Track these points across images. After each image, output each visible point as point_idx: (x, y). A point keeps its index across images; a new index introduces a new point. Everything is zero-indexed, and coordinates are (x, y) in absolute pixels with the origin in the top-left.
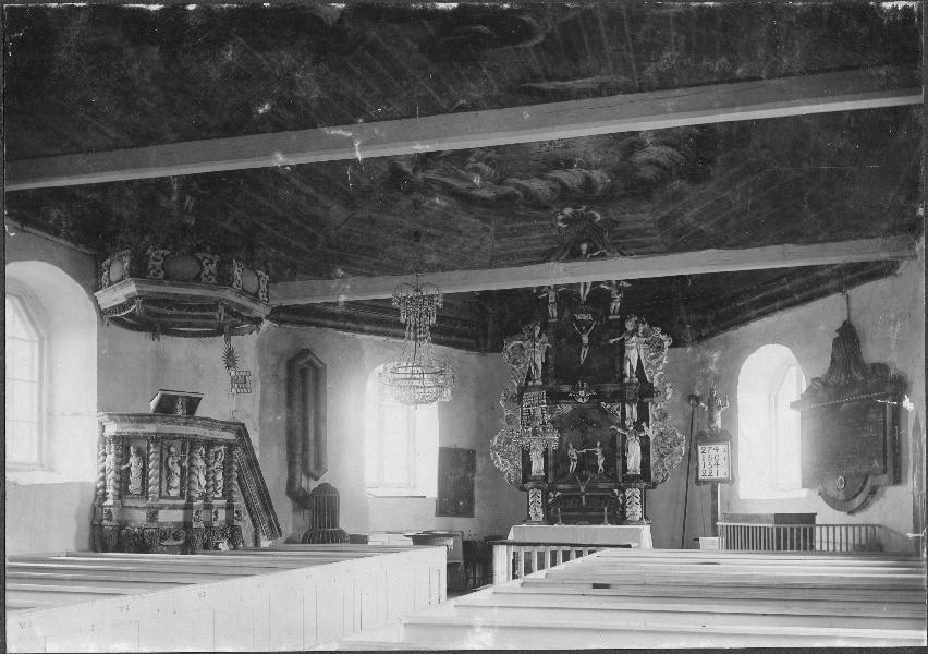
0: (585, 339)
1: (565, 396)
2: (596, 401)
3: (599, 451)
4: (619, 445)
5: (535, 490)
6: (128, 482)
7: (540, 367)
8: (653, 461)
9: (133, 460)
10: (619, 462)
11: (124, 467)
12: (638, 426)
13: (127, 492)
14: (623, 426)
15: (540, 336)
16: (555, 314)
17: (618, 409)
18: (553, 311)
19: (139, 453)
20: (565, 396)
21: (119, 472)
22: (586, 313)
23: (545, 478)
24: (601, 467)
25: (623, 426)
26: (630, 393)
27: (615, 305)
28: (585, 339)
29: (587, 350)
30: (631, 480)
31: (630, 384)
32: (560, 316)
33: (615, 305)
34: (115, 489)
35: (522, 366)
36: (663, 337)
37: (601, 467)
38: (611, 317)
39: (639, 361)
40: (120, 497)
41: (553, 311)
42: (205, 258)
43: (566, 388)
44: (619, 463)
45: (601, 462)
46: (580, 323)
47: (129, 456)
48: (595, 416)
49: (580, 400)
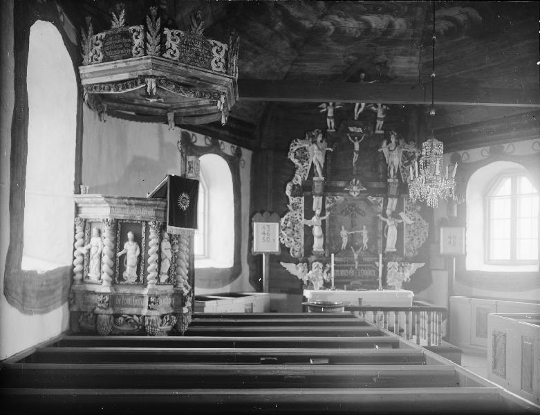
1: (341, 190)
3: (365, 233)
4: (380, 228)
5: (318, 263)
6: (122, 269)
7: (322, 165)
8: (406, 240)
9: (130, 249)
10: (380, 242)
11: (119, 254)
13: (121, 278)
14: (385, 215)
15: (321, 142)
16: (333, 125)
18: (330, 123)
19: (137, 239)
21: (114, 258)
22: (358, 127)
24: (365, 245)
25: (385, 215)
27: (380, 123)
30: (388, 257)
31: (394, 183)
33: (380, 123)
34: (108, 273)
35: (305, 164)
37: (365, 245)
38: (377, 132)
40: (113, 284)
41: (330, 123)
42: (215, 45)
44: (380, 242)
45: (365, 241)
46: (353, 135)
47: (124, 239)
49: (352, 194)
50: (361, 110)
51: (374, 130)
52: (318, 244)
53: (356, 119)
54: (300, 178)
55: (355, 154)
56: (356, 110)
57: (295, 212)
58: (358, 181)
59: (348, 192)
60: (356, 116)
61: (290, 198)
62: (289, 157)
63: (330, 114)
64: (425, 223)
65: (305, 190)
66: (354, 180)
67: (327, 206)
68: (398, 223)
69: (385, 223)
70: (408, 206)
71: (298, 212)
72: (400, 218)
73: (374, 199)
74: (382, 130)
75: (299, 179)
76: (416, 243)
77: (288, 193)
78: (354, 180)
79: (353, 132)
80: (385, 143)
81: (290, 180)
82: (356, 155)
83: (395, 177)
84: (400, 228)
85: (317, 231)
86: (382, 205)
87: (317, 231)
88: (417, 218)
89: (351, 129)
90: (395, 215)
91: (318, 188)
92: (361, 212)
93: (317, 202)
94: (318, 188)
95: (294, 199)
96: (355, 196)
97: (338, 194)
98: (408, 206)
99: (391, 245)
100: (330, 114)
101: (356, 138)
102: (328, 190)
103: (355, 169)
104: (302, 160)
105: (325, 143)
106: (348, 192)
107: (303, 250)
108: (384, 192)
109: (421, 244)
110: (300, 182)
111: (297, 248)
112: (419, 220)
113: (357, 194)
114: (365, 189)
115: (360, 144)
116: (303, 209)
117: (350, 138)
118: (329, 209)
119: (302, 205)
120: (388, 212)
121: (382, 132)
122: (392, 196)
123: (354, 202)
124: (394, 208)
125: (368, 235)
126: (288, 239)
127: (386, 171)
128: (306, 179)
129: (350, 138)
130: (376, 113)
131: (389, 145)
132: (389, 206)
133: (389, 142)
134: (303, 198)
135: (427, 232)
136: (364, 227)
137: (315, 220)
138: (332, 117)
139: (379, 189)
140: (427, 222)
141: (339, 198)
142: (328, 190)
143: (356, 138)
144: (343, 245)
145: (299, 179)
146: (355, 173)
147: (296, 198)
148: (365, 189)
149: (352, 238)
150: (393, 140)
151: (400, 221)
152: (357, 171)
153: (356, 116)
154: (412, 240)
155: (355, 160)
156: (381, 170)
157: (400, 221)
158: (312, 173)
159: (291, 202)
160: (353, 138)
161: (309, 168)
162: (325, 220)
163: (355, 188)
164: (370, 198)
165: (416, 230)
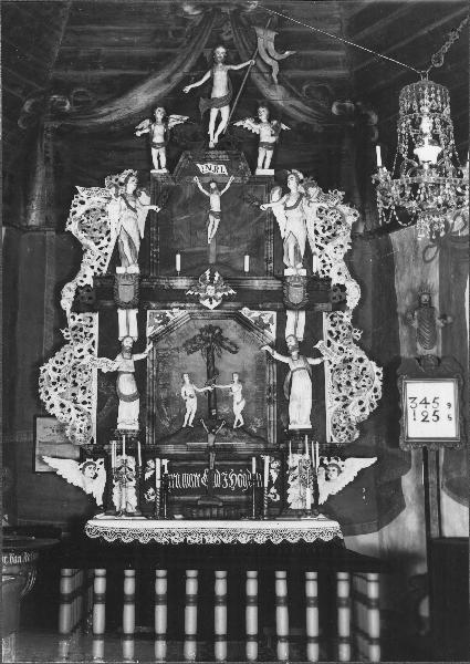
0: (215, 203)
1: (180, 296)
2: (233, 305)
8: (331, 406)
12: (307, 348)
14: (285, 352)
17: (271, 320)
18: (159, 156)
20: (180, 296)
23: (141, 435)
24: (239, 417)
26: (296, 295)
27: (265, 156)
28: (215, 203)
29: (217, 221)
32: (171, 164)
33: (265, 156)
35: (104, 243)
36: (345, 209)
37: (239, 417)
38: (259, 172)
39: (307, 243)
41: (159, 156)
43: (181, 283)
48: (232, 331)
49: (206, 303)
50: (223, 126)
51: (253, 166)
52: (128, 416)
53: (211, 145)
54: (90, 273)
55: (211, 218)
56: (211, 132)
57: (80, 346)
58: (217, 275)
59: (196, 299)
60: (214, 140)
61: (69, 314)
62: (69, 228)
63: (158, 139)
64: (373, 368)
65: (101, 298)
66: (208, 272)
67: (150, 331)
68: (312, 366)
69: (284, 369)
70: (333, 329)
71: (86, 345)
72: (318, 354)
73: (256, 314)
74: (270, 168)
75: (86, 276)
76: (355, 413)
77: (66, 304)
78: (208, 272)
79: (208, 175)
80: (276, 194)
81: (71, 277)
82: (213, 224)
83: (300, 265)
84: (317, 375)
85: (127, 386)
86: (273, 328)
87: (127, 386)
88: (357, 356)
89: (203, 168)
90: (307, 348)
91: (126, 293)
92: (227, 345)
93: (127, 322)
94: (126, 293)
95: (77, 317)
96: (211, 307)
97: (174, 304)
98: (333, 329)
99: (300, 417)
100: (158, 139)
101: (213, 185)
102: (148, 296)
103: (213, 249)
104: (97, 234)
105: (145, 198)
106: (196, 299)
107: (94, 433)
108: (278, 301)
109: (367, 412)
110: (89, 281)
111: (79, 424)
112: (361, 360)
113: (215, 304)
114: (232, 292)
115: (222, 198)
116: (96, 338)
117: (200, 187)
118: (156, 339)
119: (95, 330)
120: (291, 343)
121: (272, 172)
122: (296, 308)
123: (213, 323)
124: (300, 334)
125: (245, 394)
126: (62, 406)
127: (280, 252)
128: (105, 270)
129: (200, 187)
130: (257, 137)
131: (285, 197)
132: (289, 331)
133: (286, 191)
134: (96, 316)
135: (380, 389)
136: (236, 378)
137: (124, 363)
138: (162, 145)
139: (265, 292)
140: (378, 366)
141: (177, 314)
142: (148, 296)
143: (213, 185)
144: (187, 416)
145: (86, 276)
146: (212, 260)
147: (81, 316)
148: (232, 292)
149: (211, 401)
150: (292, 184)
151: (317, 361)
152: (218, 256)
153: (214, 140)
154: (345, 406)
155: (212, 232)
156: (270, 250)
157: (317, 361)
158: (117, 258)
159: (72, 323)
160: (207, 187)
161: (110, 250)
162: (144, 361)
163: (211, 290)
164: (245, 311)
165: (354, 383)
